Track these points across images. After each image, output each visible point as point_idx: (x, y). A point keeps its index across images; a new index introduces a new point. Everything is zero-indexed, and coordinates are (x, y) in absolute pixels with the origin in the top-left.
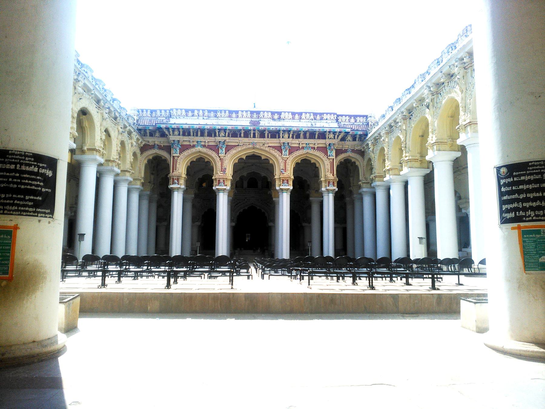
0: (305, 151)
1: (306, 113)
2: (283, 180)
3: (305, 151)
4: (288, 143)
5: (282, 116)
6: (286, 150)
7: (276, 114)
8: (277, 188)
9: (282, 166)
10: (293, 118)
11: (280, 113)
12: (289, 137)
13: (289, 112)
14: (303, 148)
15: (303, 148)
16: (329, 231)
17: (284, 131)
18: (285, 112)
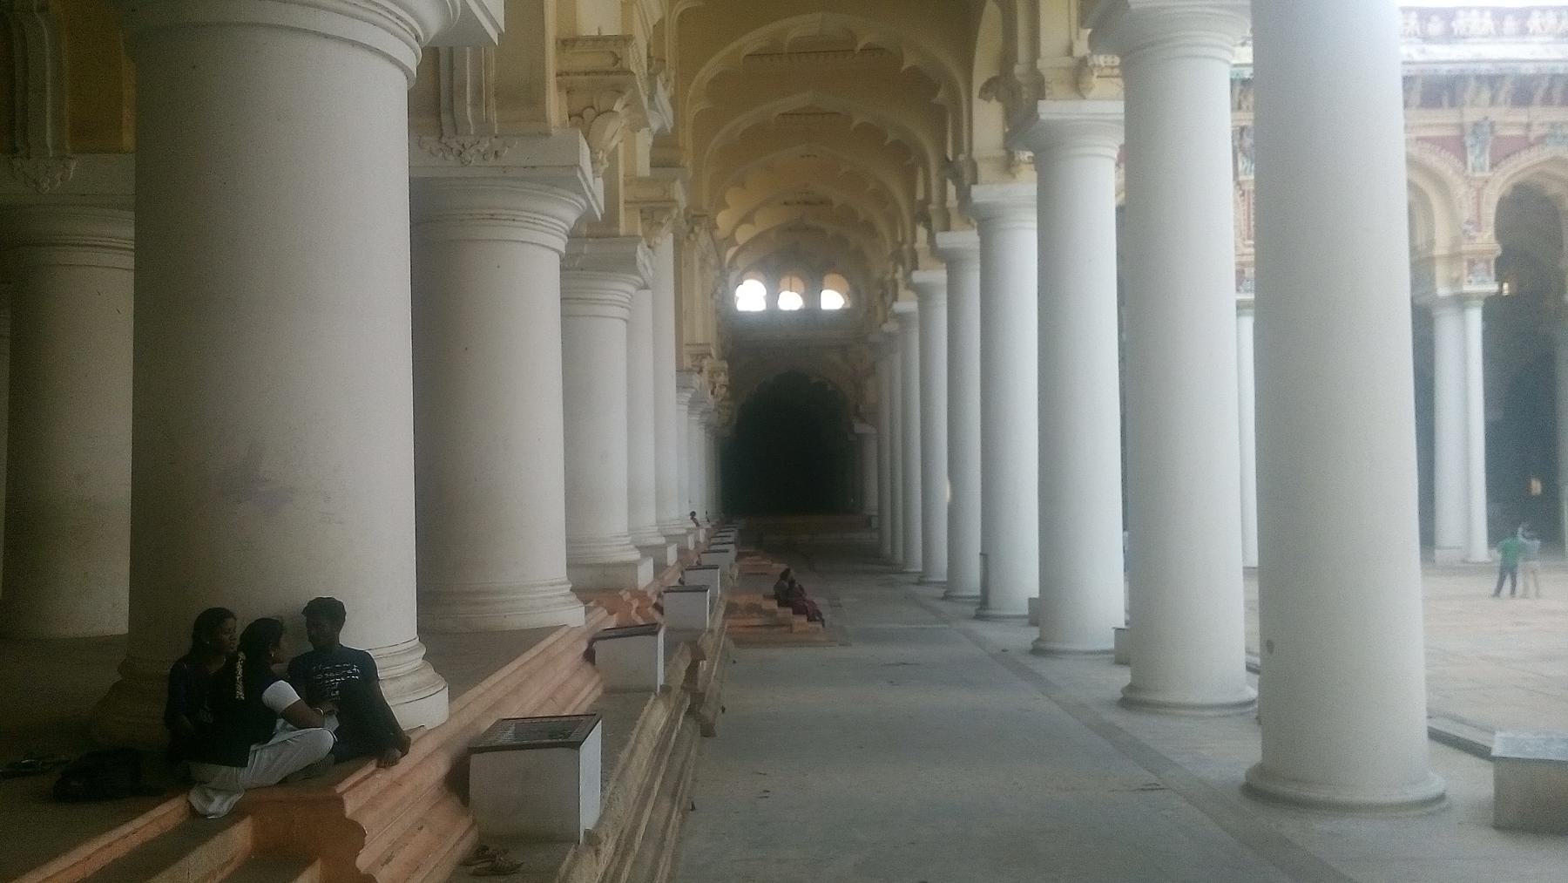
0: (1547, 152)
1: (1544, 10)
2: (1472, 263)
3: (1547, 152)
4: (1492, 125)
5: (1459, 25)
6: (1482, 151)
7: (1435, 18)
8: (1443, 291)
9: (1466, 214)
10: (1499, 33)
11: (1449, 15)
12: (1493, 101)
13: (1482, 10)
14: (1541, 140)
15: (1541, 140)
16: (1239, 366)
17: (1479, 78)
18: (1468, 10)
